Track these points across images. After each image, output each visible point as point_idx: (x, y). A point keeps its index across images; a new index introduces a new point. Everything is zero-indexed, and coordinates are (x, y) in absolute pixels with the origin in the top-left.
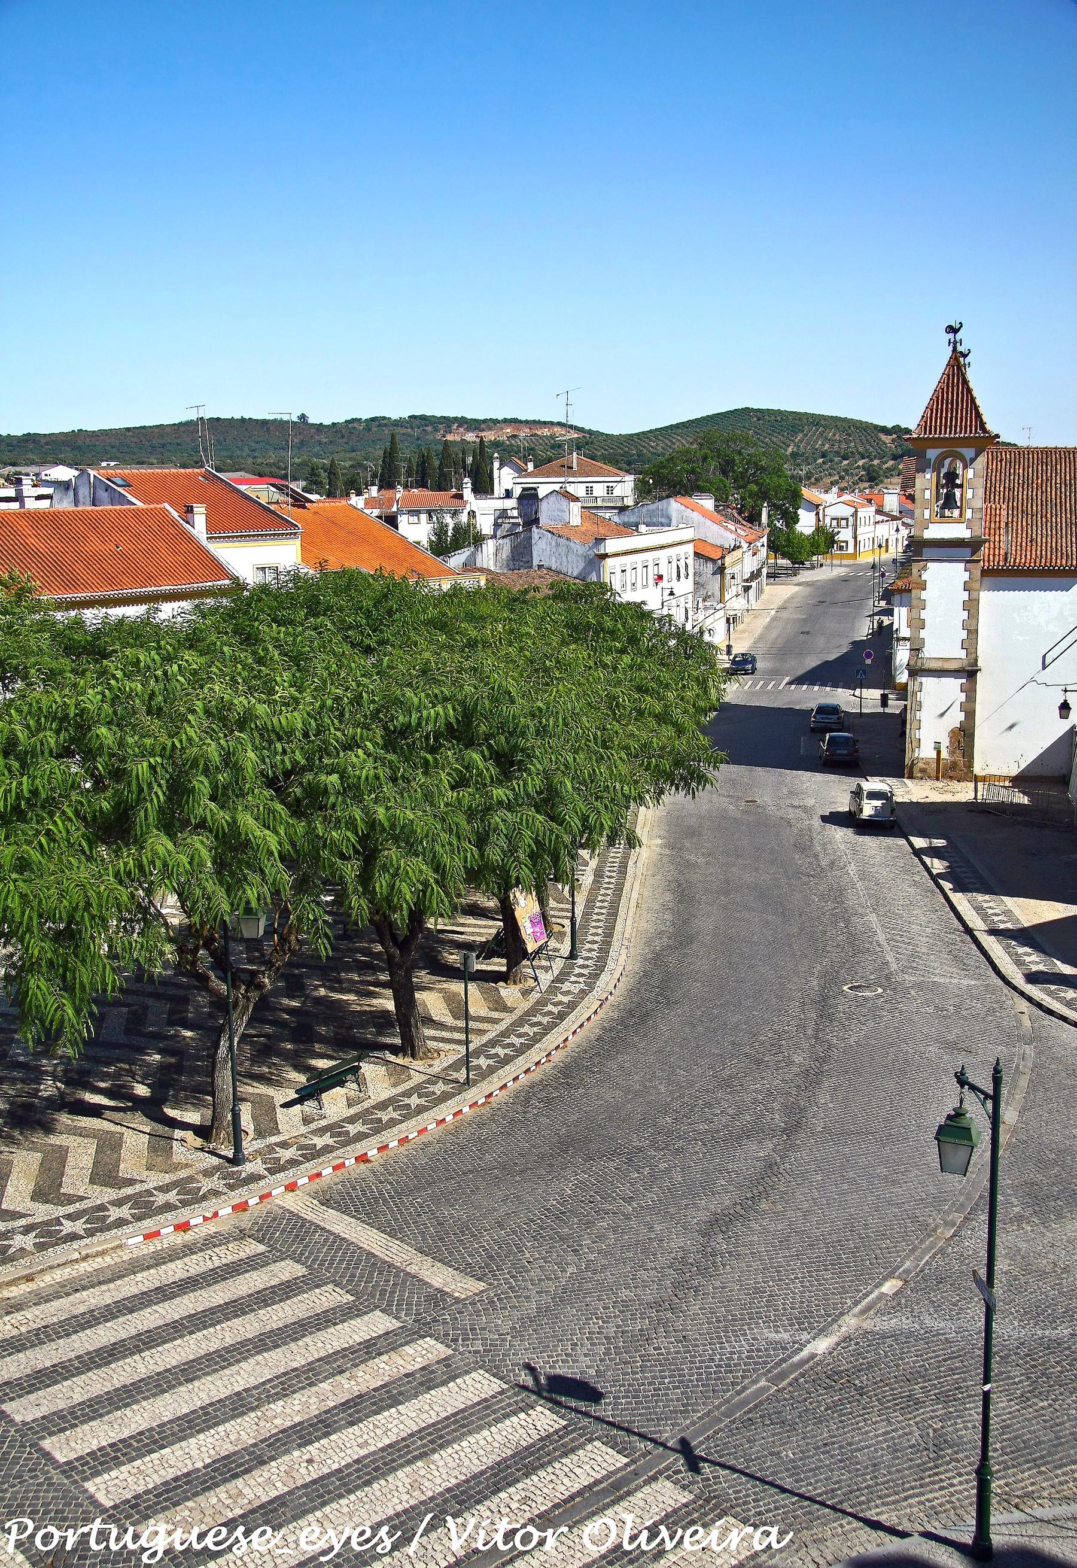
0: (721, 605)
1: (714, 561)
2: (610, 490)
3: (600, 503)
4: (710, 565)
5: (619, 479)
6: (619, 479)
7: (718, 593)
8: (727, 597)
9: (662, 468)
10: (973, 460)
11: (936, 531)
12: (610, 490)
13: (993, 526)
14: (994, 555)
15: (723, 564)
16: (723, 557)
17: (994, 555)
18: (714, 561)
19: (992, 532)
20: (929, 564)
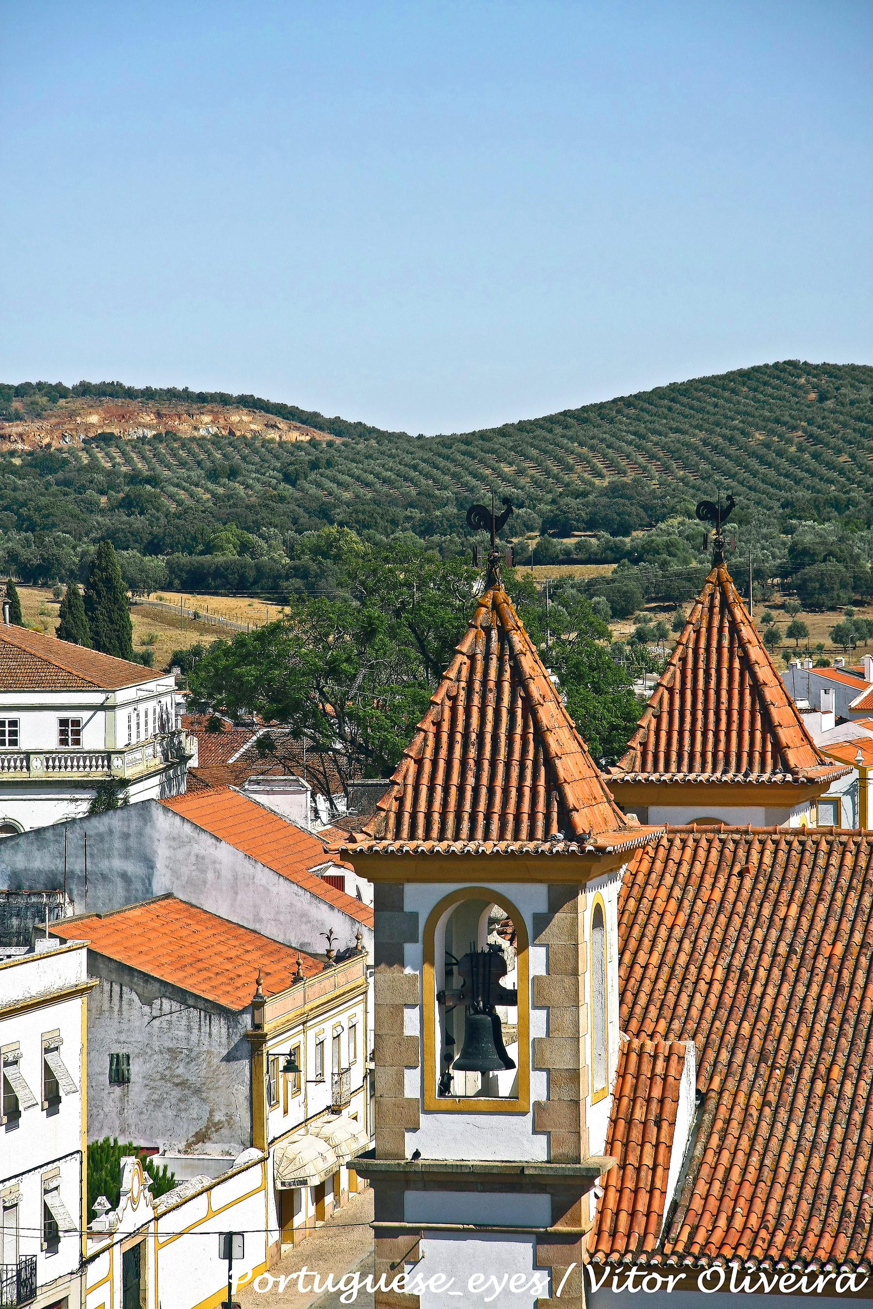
0: (254, 1154)
1: (229, 1015)
2: (70, 730)
3: (38, 770)
4: (219, 1027)
5: (97, 698)
6: (97, 698)
7: (243, 1117)
8: (276, 1122)
9: (244, 659)
10: (542, 922)
11: (443, 1141)
12: (70, 730)
13: (639, 1114)
14: (633, 1214)
15: (258, 1026)
16: (258, 1005)
17: (633, 1214)
18: (229, 1015)
19: (636, 1134)
20: (426, 1245)
